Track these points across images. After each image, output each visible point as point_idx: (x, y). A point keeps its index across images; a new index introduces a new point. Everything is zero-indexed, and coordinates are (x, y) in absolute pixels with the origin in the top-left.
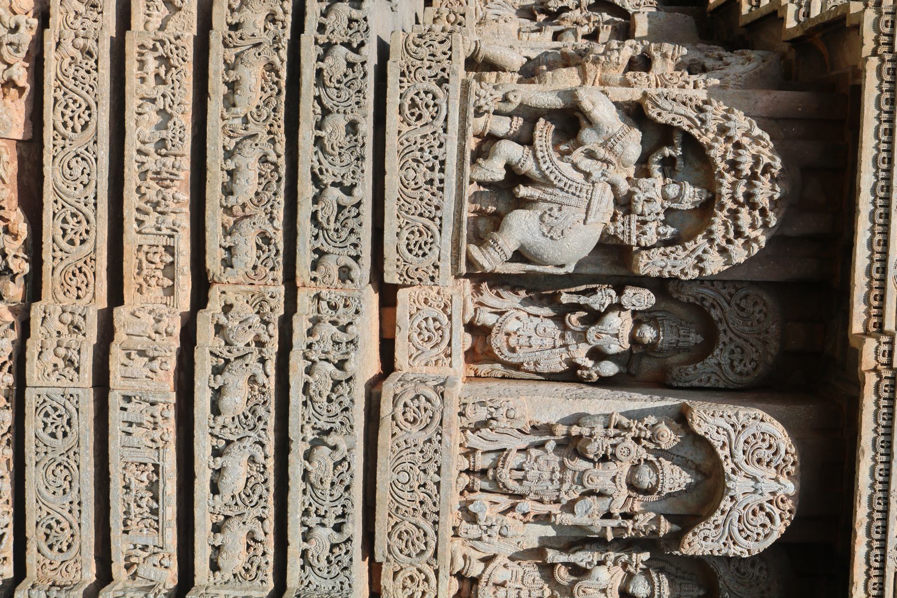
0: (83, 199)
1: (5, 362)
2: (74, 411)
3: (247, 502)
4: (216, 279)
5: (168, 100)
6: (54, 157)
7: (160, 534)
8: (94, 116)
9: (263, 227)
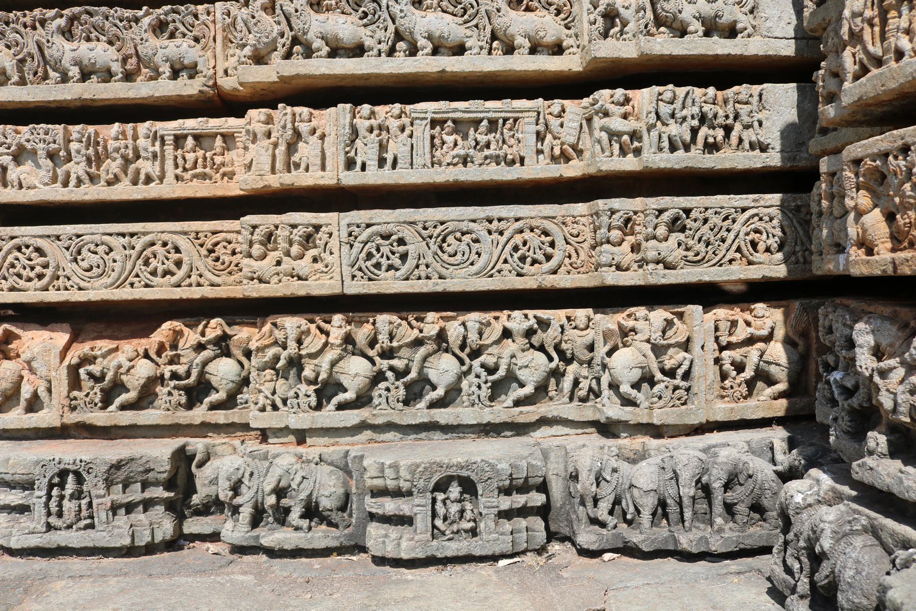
0: (127, 252)
4: (211, 83)
6: (80, 289)
7: (520, 115)
9: (145, 27)
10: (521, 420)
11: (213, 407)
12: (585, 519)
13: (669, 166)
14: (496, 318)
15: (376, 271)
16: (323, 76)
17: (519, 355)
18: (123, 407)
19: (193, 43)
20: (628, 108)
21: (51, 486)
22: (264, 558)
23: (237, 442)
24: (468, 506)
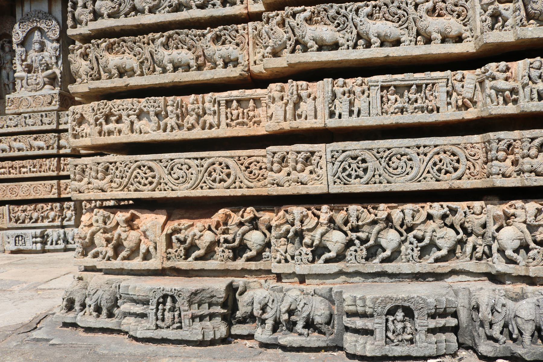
0: (199, 169)
1: (313, 213)
2: (344, 154)
3: (403, 19)
4: (246, 69)
5: (131, 112)
6: (173, 190)
7: (436, 81)
8: (144, 162)
10: (439, 271)
11: (249, 260)
12: (483, 336)
13: (538, 110)
14: (423, 207)
15: (349, 179)
16: (315, 62)
17: (438, 230)
18: (196, 259)
19: (236, 47)
20: (508, 74)
21: (158, 304)
22: (280, 351)
23: (262, 281)
24: (408, 325)
